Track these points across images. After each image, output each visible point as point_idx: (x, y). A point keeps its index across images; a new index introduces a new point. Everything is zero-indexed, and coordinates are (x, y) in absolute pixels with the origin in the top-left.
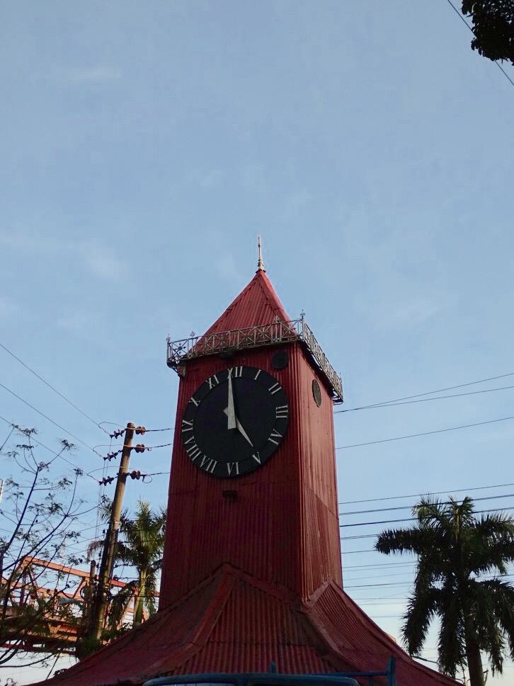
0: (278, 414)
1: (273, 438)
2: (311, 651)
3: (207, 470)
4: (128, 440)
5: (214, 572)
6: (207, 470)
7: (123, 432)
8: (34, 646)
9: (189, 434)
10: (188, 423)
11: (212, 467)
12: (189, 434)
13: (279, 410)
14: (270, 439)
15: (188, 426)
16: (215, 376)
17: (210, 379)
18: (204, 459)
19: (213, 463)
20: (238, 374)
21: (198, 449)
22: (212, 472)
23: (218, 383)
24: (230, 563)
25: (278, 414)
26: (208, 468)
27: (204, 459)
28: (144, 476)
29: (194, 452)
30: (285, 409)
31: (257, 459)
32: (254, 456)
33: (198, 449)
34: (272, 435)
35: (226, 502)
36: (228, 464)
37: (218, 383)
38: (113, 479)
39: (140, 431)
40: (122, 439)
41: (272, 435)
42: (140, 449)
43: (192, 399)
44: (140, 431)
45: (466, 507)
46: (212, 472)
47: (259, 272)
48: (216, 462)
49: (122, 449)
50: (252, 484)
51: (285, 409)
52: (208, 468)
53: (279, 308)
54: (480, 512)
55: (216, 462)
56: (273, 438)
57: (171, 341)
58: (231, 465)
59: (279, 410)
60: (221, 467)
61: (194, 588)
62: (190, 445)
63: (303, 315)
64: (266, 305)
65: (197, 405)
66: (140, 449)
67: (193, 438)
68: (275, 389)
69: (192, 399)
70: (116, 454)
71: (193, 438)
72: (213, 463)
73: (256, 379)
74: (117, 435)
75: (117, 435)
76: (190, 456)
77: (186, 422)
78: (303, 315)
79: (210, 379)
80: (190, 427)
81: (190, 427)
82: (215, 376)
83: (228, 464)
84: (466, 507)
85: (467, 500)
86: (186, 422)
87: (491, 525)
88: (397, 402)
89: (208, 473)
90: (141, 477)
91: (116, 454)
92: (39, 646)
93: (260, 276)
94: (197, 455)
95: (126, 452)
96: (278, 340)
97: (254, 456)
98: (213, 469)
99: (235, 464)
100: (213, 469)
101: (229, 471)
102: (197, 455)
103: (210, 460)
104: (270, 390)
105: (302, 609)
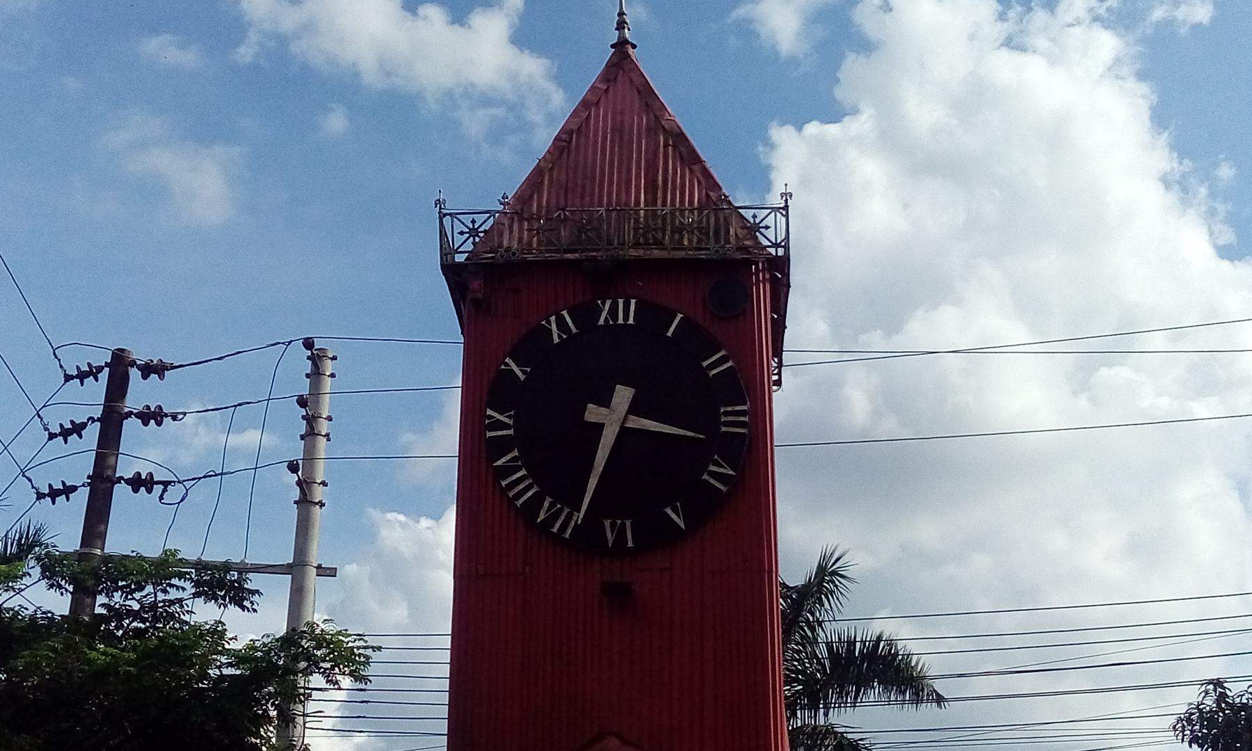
0: (727, 424)
4: (117, 389)
9: (502, 446)
12: (502, 446)
13: (727, 413)
16: (565, 313)
17: (553, 319)
18: (546, 504)
20: (626, 317)
23: (574, 330)
25: (727, 424)
27: (546, 504)
30: (743, 413)
36: (607, 523)
37: (574, 330)
40: (97, 390)
42: (152, 416)
43: (507, 360)
49: (98, 415)
51: (743, 413)
59: (727, 413)
65: (522, 377)
66: (152, 416)
67: (516, 453)
68: (716, 364)
70: (84, 425)
71: (516, 453)
73: (669, 334)
74: (82, 376)
76: (511, 494)
79: (553, 319)
80: (507, 426)
81: (507, 426)
82: (565, 313)
83: (607, 523)
91: (84, 425)
94: (530, 494)
99: (623, 525)
102: (530, 494)
104: (705, 364)
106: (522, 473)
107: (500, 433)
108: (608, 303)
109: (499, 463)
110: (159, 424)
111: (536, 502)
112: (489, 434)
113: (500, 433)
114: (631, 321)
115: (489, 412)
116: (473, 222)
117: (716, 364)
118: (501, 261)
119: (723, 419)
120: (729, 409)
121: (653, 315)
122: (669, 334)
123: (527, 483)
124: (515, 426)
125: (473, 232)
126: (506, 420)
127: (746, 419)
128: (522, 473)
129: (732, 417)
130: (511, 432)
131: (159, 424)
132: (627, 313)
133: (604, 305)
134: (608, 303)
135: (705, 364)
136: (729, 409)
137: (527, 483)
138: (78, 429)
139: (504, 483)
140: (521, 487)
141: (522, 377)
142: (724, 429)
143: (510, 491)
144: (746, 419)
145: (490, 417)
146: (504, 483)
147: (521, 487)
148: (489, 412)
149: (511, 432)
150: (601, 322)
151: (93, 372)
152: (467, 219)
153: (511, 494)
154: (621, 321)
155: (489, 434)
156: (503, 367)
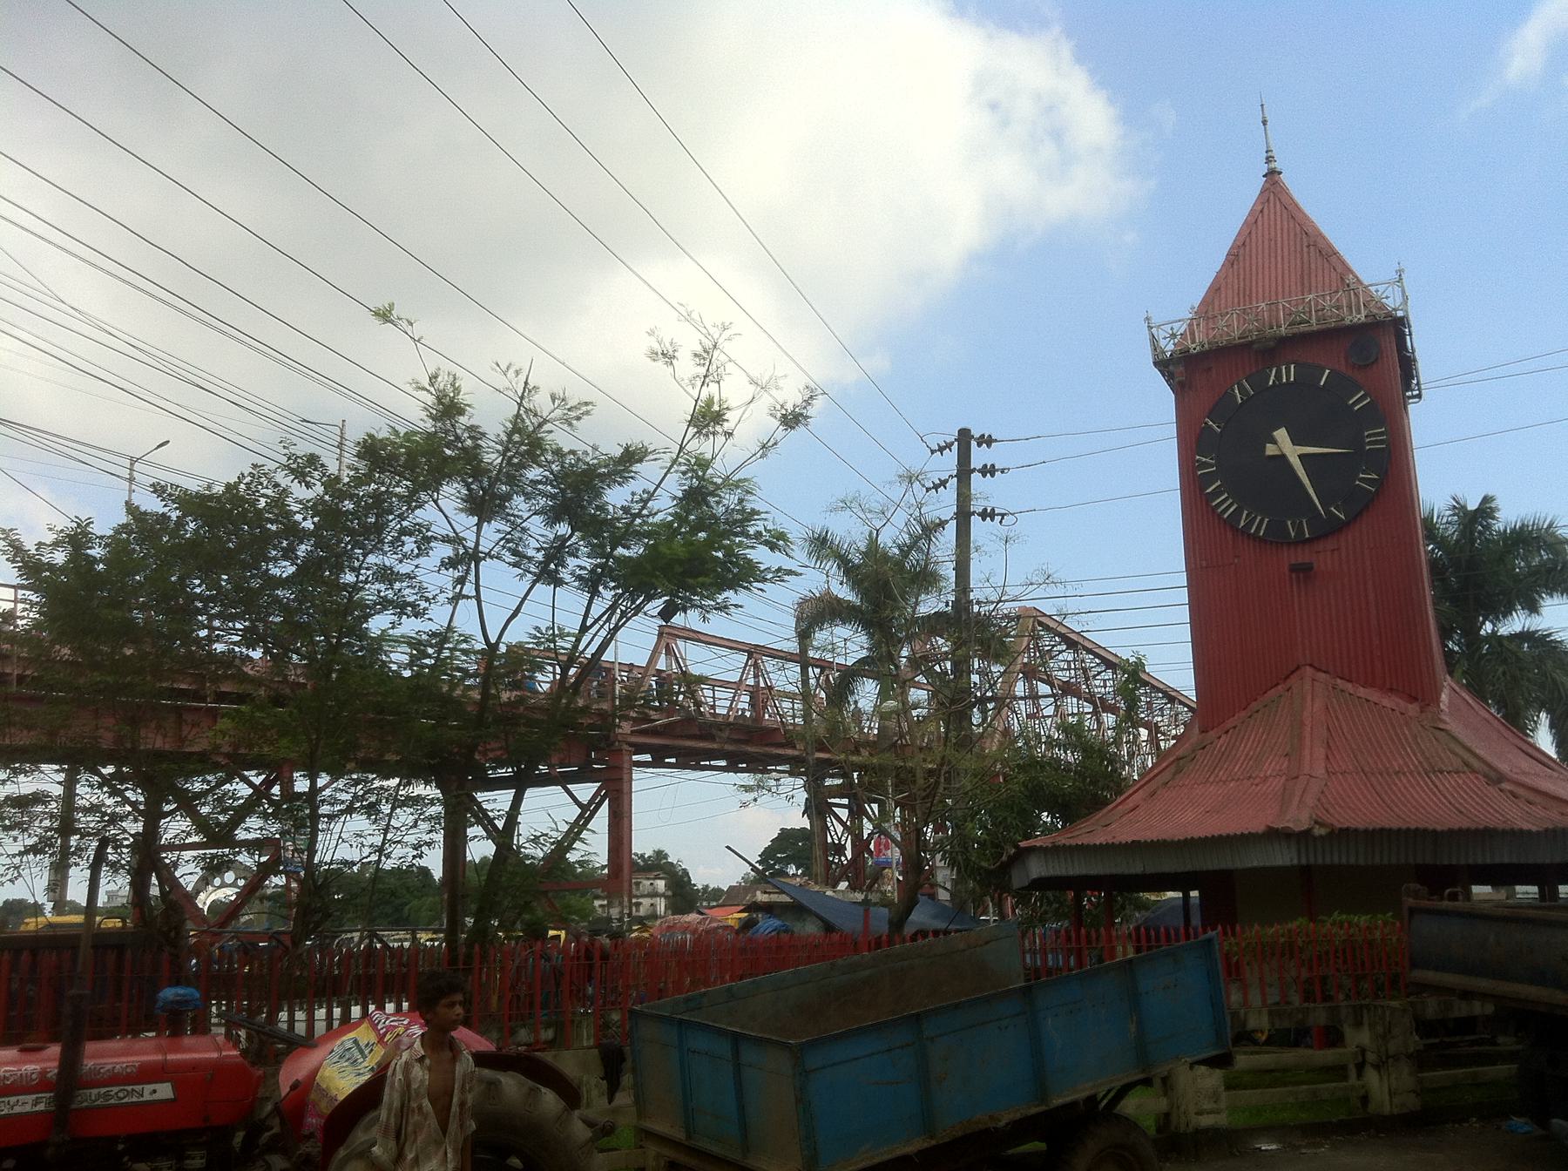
0: (1370, 443)
2: (1477, 778)
5: (1287, 677)
7: (952, 444)
8: (667, 760)
11: (1260, 525)
12: (1209, 479)
15: (1205, 465)
21: (1231, 501)
24: (1311, 665)
25: (1370, 443)
26: (1254, 527)
28: (1003, 515)
29: (1226, 505)
33: (1231, 501)
35: (1291, 578)
38: (947, 522)
39: (986, 441)
41: (1361, 476)
42: (988, 471)
44: (986, 441)
45: (1486, 509)
47: (1272, 174)
49: (955, 472)
50: (1333, 550)
52: (1254, 527)
53: (1336, 253)
54: (1508, 516)
56: (1362, 480)
57: (1154, 321)
60: (1277, 529)
61: (1256, 700)
62: (1217, 493)
63: (1400, 273)
64: (1308, 246)
66: (988, 471)
68: (1358, 401)
70: (947, 481)
73: (1322, 383)
74: (941, 449)
75: (941, 449)
76: (1219, 510)
78: (1400, 273)
84: (1486, 509)
85: (1487, 500)
86: (1204, 459)
87: (1526, 538)
88: (1486, 374)
89: (1255, 537)
90: (998, 518)
92: (673, 760)
93: (1275, 183)
94: (1232, 510)
95: (964, 472)
96: (1361, 317)
102: (1232, 510)
103: (1255, 518)
105: (1442, 726)
106: (1226, 495)
109: (1209, 491)
110: (992, 476)
116: (1172, 329)
117: (1358, 401)
123: (1228, 502)
125: (1173, 336)
129: (1373, 437)
131: (992, 476)
132: (1289, 374)
137: (1228, 502)
138: (943, 483)
145: (1198, 461)
151: (949, 446)
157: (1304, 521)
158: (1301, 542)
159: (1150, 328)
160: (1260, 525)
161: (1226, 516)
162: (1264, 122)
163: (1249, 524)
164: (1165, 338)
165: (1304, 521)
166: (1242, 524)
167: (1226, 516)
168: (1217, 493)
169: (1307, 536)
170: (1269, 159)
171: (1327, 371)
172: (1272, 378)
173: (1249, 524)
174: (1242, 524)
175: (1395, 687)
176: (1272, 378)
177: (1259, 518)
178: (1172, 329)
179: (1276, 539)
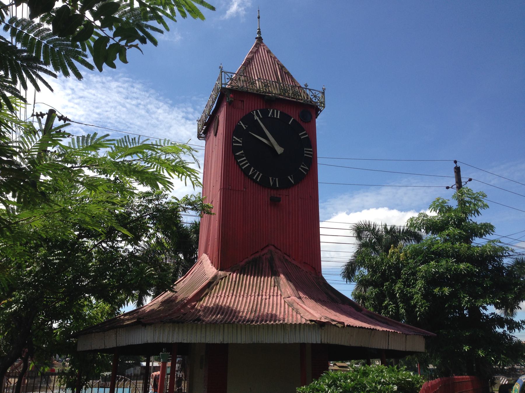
0: (306, 153)
1: (302, 168)
3: (254, 178)
6: (254, 178)
7: (44, 115)
9: (238, 149)
10: (238, 140)
12: (238, 149)
13: (306, 150)
14: (300, 169)
16: (258, 111)
18: (252, 170)
19: (259, 175)
21: (246, 161)
22: (258, 180)
24: (274, 246)
25: (306, 153)
26: (255, 176)
27: (252, 170)
30: (311, 151)
31: (291, 179)
32: (289, 177)
33: (246, 161)
34: (302, 166)
41: (302, 166)
43: (240, 122)
46: (258, 180)
48: (261, 174)
50: (286, 196)
51: (311, 151)
52: (255, 176)
55: (261, 174)
56: (302, 168)
58: (272, 179)
59: (306, 150)
61: (247, 258)
62: (240, 157)
65: (245, 128)
69: (240, 122)
72: (259, 175)
73: (290, 123)
76: (241, 164)
77: (237, 139)
78: (324, 90)
80: (239, 143)
81: (239, 143)
82: (258, 111)
86: (237, 139)
89: (255, 181)
94: (247, 165)
97: (289, 177)
98: (259, 179)
100: (259, 179)
101: (271, 184)
102: (247, 165)
103: (256, 172)
104: (300, 134)
106: (245, 158)
107: (237, 145)
108: (272, 110)
111: (249, 168)
112: (234, 144)
113: (237, 145)
114: (278, 117)
115: (234, 137)
118: (240, 90)
119: (305, 152)
120: (307, 149)
121: (285, 117)
122: (290, 123)
124: (242, 143)
126: (240, 141)
127: (312, 153)
128: (245, 158)
130: (241, 145)
133: (270, 111)
134: (272, 110)
135: (300, 134)
136: (307, 149)
139: (239, 161)
140: (244, 163)
141: (245, 128)
142: (305, 155)
143: (241, 163)
144: (312, 153)
146: (239, 161)
147: (244, 163)
148: (234, 137)
149: (241, 145)
150: (269, 116)
152: (230, 75)
153: (241, 164)
154: (275, 116)
155: (234, 144)
156: (239, 124)
157: (277, 179)
158: (274, 188)
159: (222, 72)
160: (258, 176)
161: (243, 168)
162: (259, 18)
163: (254, 174)
164: (228, 79)
165: (277, 179)
166: (250, 173)
167: (243, 168)
168: (240, 157)
169: (277, 186)
170: (259, 33)
171: (293, 119)
172: (270, 113)
173: (254, 174)
174: (250, 173)
175: (306, 262)
176: (270, 113)
177: (258, 172)
178: (232, 76)
179: (264, 184)
